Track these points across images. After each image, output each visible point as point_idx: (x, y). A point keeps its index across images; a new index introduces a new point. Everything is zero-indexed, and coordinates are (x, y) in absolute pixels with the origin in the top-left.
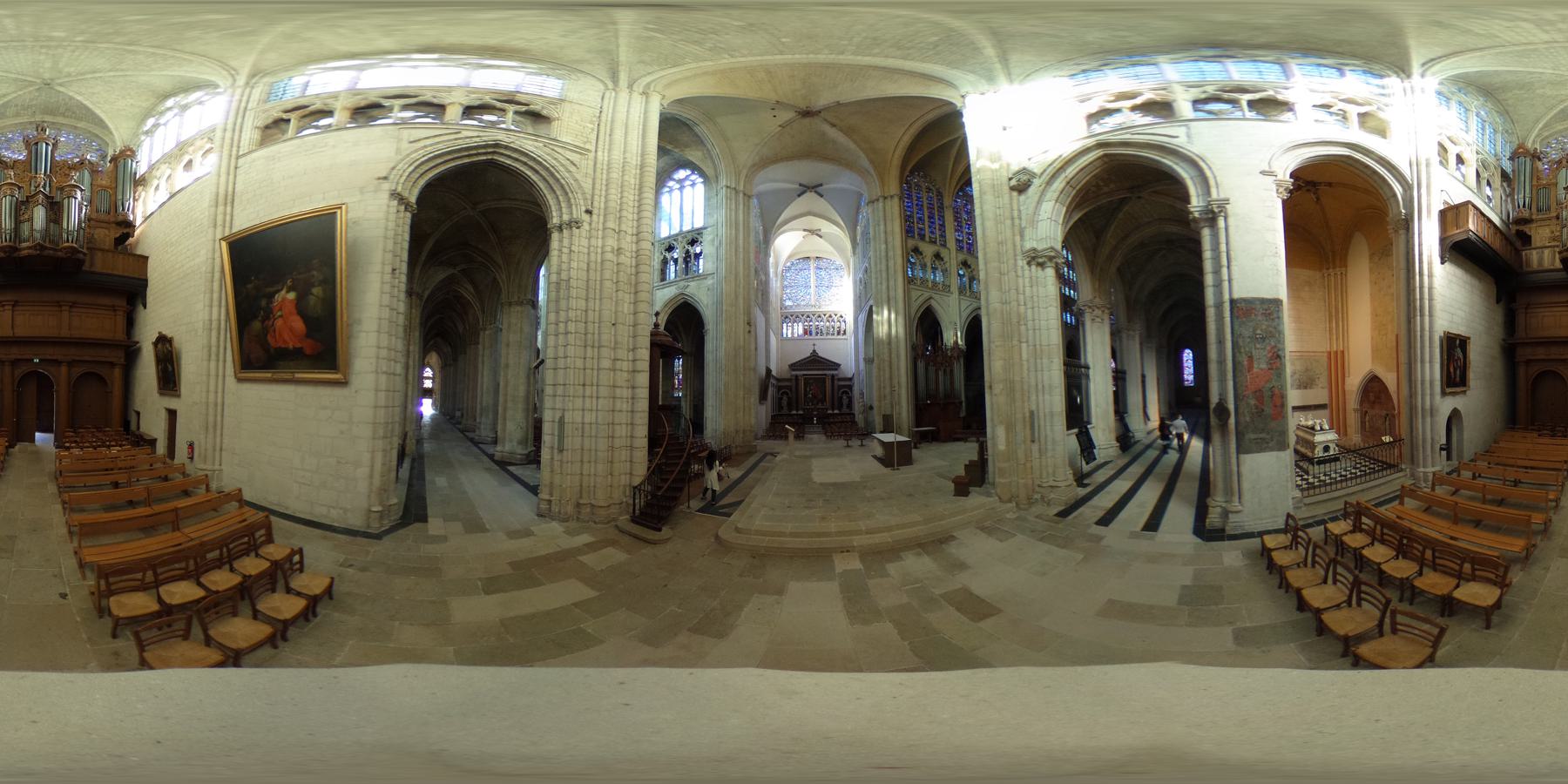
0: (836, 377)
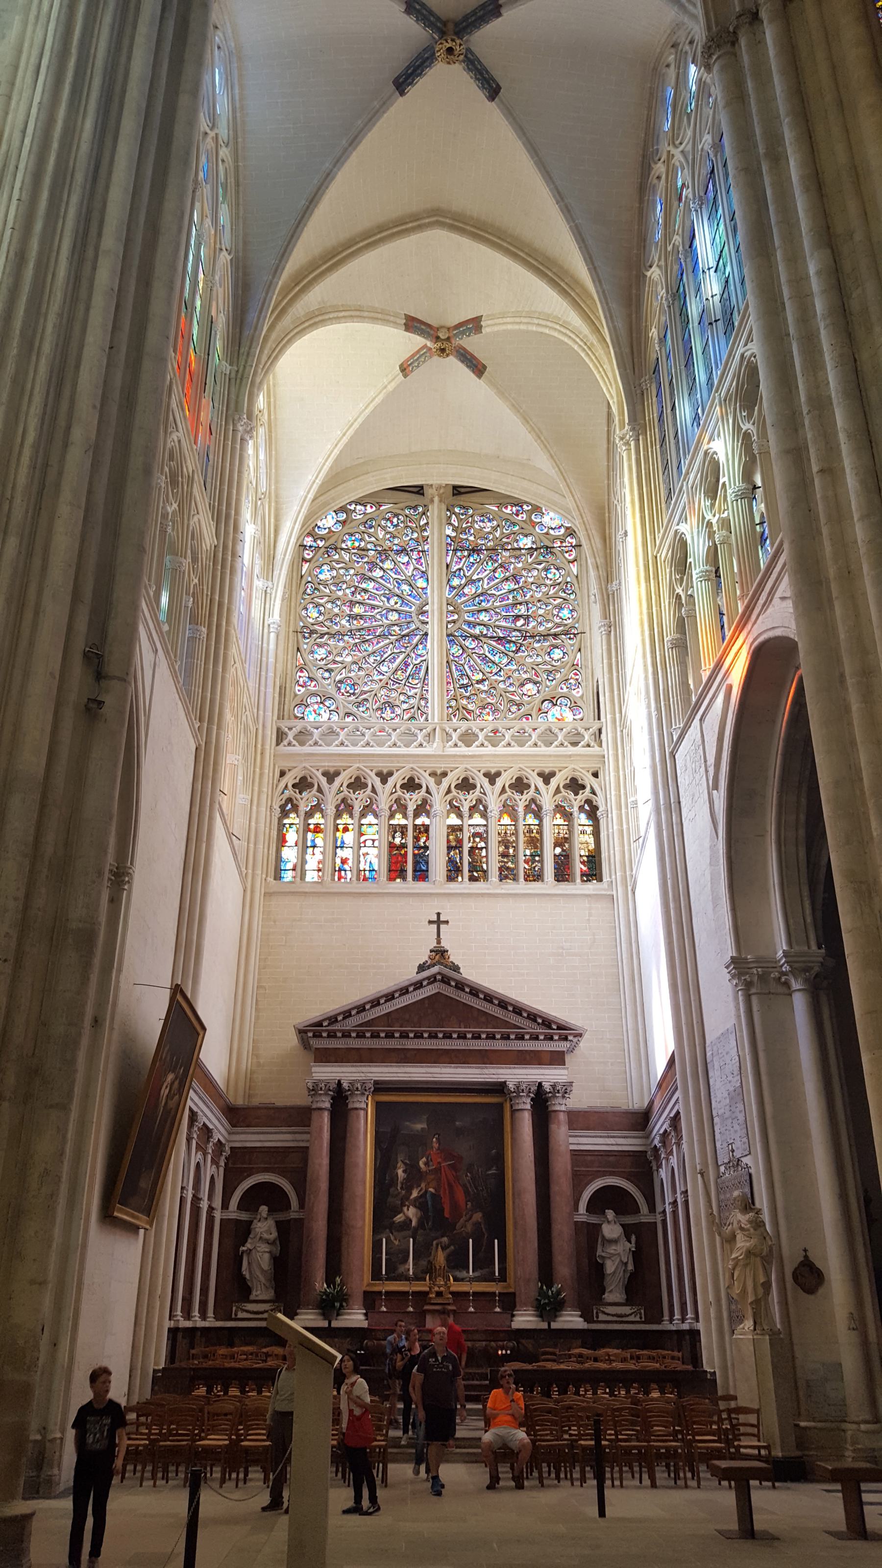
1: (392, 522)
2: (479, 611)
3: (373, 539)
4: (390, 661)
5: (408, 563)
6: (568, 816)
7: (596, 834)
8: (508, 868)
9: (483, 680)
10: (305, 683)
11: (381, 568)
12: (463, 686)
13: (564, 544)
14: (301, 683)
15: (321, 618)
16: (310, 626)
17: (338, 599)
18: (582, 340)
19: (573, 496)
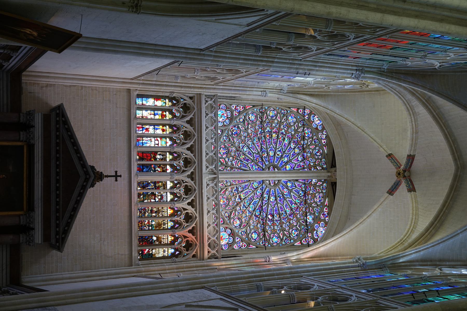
0: (22, 238)
1: (318, 152)
2: (275, 196)
4: (249, 152)
5: (298, 160)
6: (172, 243)
7: (164, 257)
8: (145, 213)
9: (241, 199)
10: (237, 109)
11: (295, 148)
12: (237, 189)
13: (309, 238)
15: (270, 118)
17: (280, 126)
18: (405, 239)
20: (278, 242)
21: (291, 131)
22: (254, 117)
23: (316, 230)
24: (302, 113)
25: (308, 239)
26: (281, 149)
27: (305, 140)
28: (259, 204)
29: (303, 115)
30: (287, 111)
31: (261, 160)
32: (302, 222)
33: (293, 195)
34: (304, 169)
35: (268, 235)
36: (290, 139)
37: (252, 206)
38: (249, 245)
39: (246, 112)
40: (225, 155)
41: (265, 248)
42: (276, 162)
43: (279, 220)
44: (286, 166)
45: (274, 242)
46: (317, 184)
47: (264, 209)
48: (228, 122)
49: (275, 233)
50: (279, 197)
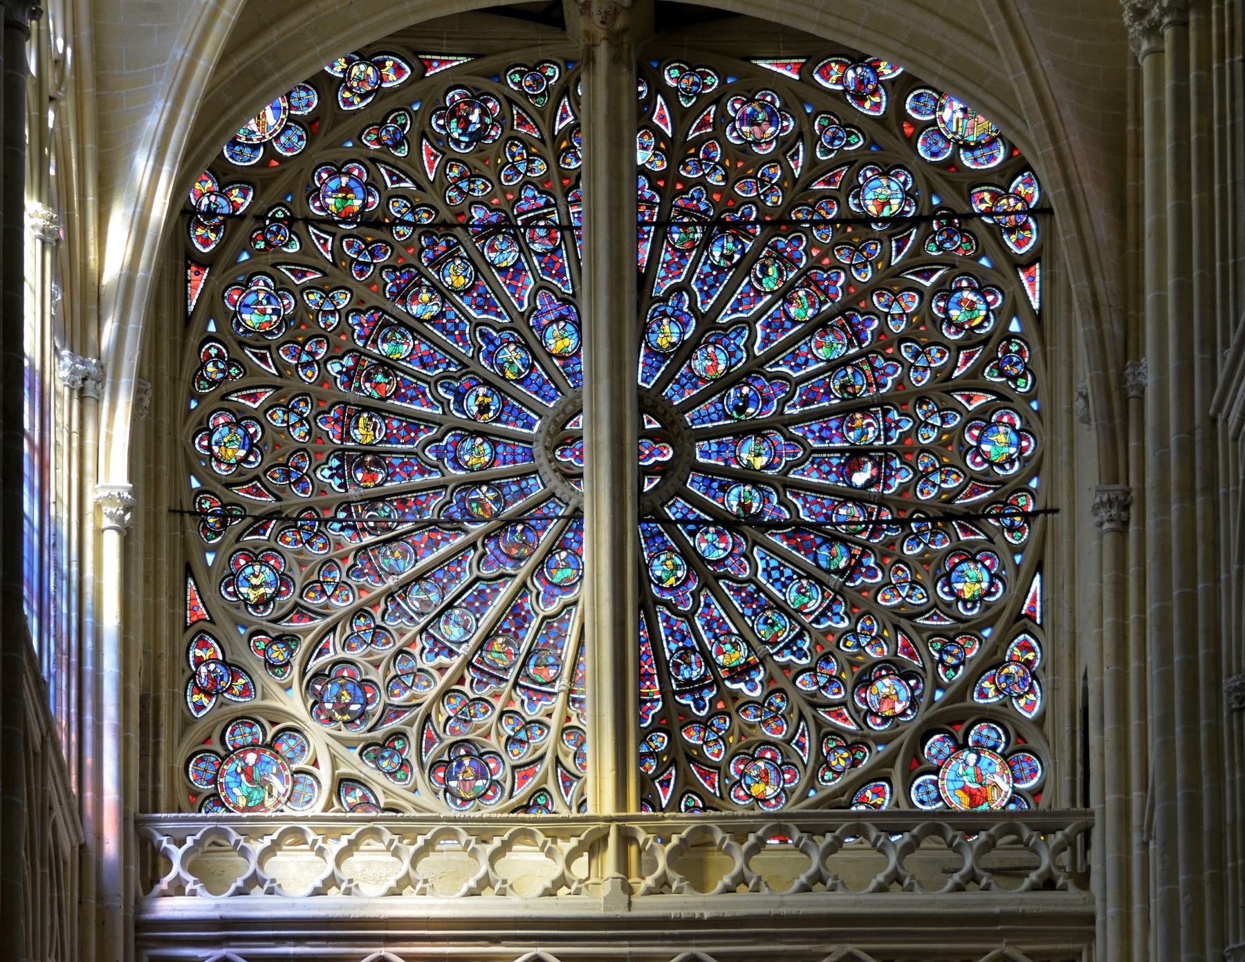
2: (740, 433)
3: (409, 184)
5: (517, 268)
10: (214, 679)
11: (435, 288)
12: (690, 687)
14: (203, 680)
16: (219, 489)
17: (304, 395)
19: (1028, 65)
20: (1013, 426)
21: (332, 313)
22: (257, 568)
23: (955, 156)
24: (216, 230)
25: (1005, 213)
26: (448, 390)
27: (387, 213)
28: (784, 545)
29: (229, 222)
30: (211, 338)
31: (520, 528)
32: (899, 251)
33: (734, 311)
34: (570, 228)
35: (973, 493)
36: (386, 324)
37: (794, 594)
38: (1020, 621)
39: (229, 626)
40: (492, 765)
41: (1046, 511)
42: (530, 426)
43: (886, 413)
44: (550, 355)
45: (1013, 450)
46: (669, 132)
47: (811, 512)
48: (292, 742)
49: (962, 442)
50: (741, 410)
